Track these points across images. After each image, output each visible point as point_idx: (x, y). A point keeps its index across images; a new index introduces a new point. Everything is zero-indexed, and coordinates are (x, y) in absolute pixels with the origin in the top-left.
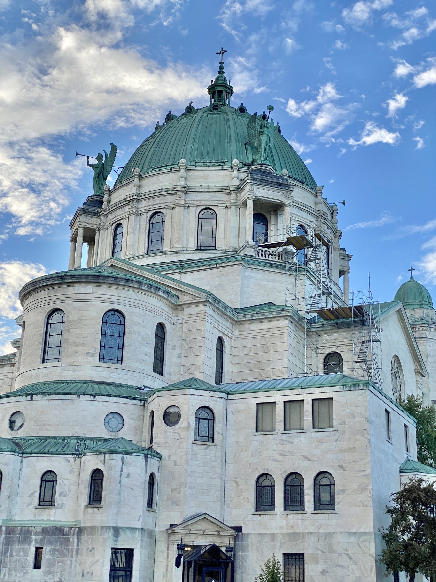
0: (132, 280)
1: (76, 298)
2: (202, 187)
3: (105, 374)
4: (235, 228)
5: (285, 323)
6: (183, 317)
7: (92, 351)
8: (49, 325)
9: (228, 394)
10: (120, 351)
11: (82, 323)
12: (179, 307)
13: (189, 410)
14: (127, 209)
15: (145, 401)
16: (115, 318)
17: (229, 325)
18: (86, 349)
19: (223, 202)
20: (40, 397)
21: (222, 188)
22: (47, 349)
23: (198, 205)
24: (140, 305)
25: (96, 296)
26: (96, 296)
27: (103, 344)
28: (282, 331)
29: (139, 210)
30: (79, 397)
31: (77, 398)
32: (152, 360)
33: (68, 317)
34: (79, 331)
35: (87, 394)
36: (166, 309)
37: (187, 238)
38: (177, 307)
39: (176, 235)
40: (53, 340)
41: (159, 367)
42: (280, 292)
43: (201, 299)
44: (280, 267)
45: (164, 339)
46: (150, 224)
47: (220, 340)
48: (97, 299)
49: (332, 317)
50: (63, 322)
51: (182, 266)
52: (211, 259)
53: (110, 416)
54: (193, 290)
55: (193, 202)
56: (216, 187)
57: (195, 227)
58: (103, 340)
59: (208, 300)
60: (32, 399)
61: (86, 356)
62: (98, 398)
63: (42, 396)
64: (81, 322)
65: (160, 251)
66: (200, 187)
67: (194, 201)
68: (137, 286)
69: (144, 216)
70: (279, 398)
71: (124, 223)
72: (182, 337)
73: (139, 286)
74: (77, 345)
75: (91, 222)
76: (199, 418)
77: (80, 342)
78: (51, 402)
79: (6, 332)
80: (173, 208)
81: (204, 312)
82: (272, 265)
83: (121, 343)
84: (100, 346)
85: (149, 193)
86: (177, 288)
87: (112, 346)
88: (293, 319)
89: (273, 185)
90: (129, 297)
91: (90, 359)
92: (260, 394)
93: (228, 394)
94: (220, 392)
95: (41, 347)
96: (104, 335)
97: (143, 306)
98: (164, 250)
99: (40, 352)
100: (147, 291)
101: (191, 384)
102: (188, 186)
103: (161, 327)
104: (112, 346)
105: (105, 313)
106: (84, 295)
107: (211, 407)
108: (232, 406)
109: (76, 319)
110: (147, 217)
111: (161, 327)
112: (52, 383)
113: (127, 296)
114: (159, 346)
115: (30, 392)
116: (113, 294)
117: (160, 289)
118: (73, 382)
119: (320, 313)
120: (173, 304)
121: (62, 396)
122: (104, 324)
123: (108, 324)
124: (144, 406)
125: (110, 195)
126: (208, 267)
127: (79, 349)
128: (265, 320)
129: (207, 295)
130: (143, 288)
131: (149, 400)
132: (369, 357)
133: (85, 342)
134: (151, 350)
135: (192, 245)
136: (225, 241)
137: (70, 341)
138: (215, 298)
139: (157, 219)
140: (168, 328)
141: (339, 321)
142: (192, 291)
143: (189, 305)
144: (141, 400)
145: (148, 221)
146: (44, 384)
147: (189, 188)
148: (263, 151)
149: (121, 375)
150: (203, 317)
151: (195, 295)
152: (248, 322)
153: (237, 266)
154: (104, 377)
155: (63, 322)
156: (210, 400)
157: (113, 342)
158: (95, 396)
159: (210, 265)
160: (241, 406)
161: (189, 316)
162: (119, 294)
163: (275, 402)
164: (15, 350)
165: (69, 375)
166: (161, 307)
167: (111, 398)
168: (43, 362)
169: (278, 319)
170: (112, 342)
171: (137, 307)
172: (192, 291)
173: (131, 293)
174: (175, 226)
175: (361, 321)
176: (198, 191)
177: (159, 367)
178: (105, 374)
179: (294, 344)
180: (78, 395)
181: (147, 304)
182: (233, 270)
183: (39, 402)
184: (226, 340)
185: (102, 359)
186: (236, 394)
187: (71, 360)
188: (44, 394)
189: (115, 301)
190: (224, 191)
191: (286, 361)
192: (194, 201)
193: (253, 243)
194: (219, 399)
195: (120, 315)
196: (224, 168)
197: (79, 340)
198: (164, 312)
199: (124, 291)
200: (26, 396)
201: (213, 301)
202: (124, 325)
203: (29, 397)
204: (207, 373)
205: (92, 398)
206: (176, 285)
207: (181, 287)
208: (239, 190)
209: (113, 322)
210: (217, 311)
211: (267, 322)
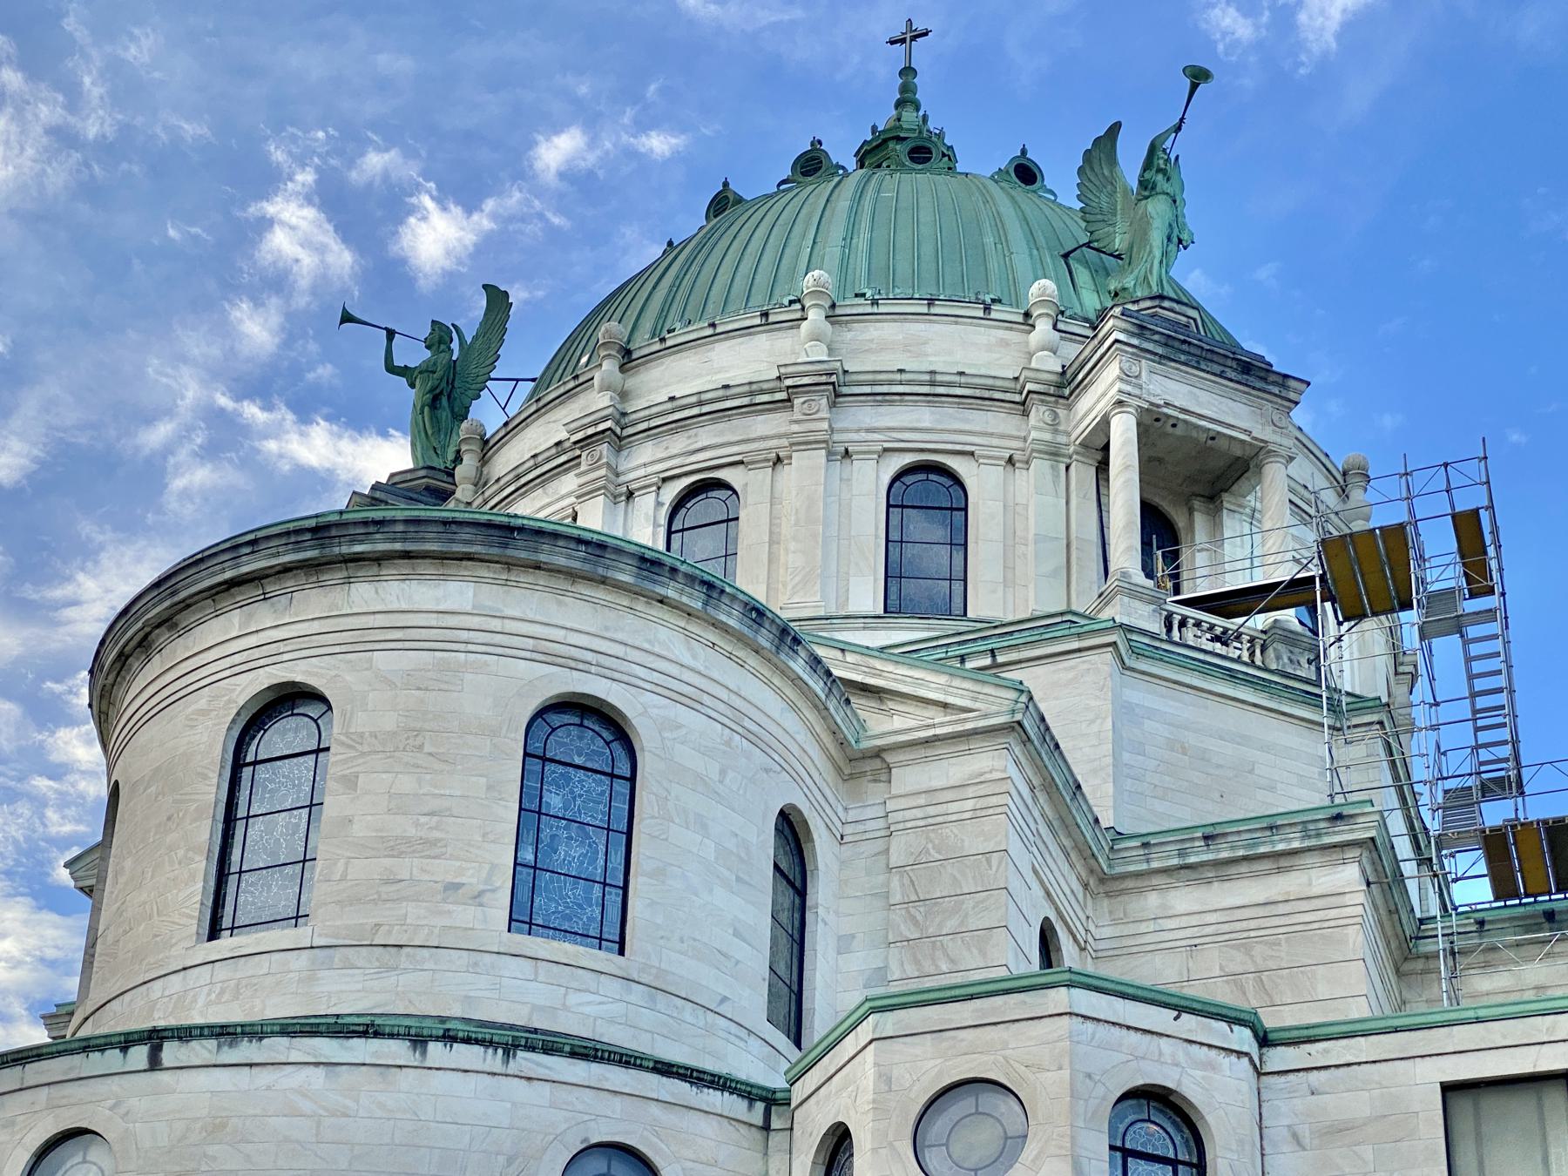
0: (674, 570)
1: (401, 634)
2: (905, 377)
6: (891, 806)
7: (474, 881)
11: (421, 747)
18: (443, 870)
19: (995, 442)
20: (202, 1050)
21: (990, 382)
22: (233, 879)
23: (886, 450)
24: (706, 699)
25: (495, 624)
26: (495, 624)
27: (528, 856)
29: (622, 479)
30: (424, 1053)
34: (406, 783)
35: (467, 1041)
43: (986, 716)
45: (802, 893)
46: (670, 533)
48: (498, 639)
50: (318, 751)
54: (943, 679)
55: (864, 436)
56: (963, 379)
57: (877, 537)
59: (1018, 717)
60: (155, 1064)
61: (444, 901)
62: (525, 1061)
64: (417, 743)
66: (898, 377)
67: (868, 430)
69: (645, 502)
72: (887, 895)
73: (706, 604)
76: (1127, 1153)
77: (412, 832)
78: (264, 1077)
80: (779, 460)
83: (617, 859)
84: (516, 864)
85: (669, 406)
86: (859, 678)
89: (1217, 369)
90: (657, 650)
91: (465, 915)
96: (531, 813)
97: (721, 707)
100: (740, 638)
102: (846, 372)
105: (541, 713)
108: (1290, 1104)
110: (659, 504)
113: (646, 646)
116: (576, 626)
120: (843, 744)
121: (326, 1047)
122: (535, 765)
123: (549, 767)
124: (766, 1127)
125: (484, 460)
127: (406, 867)
129: (1013, 695)
130: (723, 618)
133: (436, 834)
137: (358, 830)
140: (823, 850)
143: (922, 752)
145: (663, 520)
147: (848, 378)
148: (1157, 253)
150: (994, 800)
151: (950, 700)
154: (535, 1008)
155: (318, 751)
156: (1181, 1057)
158: (510, 1049)
161: (922, 800)
162: (607, 629)
170: (570, 853)
173: (663, 634)
174: (786, 529)
176: (885, 392)
180: (419, 1041)
181: (738, 703)
182: (1071, 675)
185: (522, 919)
189: (589, 656)
190: (997, 395)
192: (868, 430)
196: (993, 315)
197: (404, 826)
198: (808, 764)
200: (124, 1050)
202: (632, 779)
203: (140, 1054)
205: (494, 1060)
208: (1067, 392)
209: (578, 761)
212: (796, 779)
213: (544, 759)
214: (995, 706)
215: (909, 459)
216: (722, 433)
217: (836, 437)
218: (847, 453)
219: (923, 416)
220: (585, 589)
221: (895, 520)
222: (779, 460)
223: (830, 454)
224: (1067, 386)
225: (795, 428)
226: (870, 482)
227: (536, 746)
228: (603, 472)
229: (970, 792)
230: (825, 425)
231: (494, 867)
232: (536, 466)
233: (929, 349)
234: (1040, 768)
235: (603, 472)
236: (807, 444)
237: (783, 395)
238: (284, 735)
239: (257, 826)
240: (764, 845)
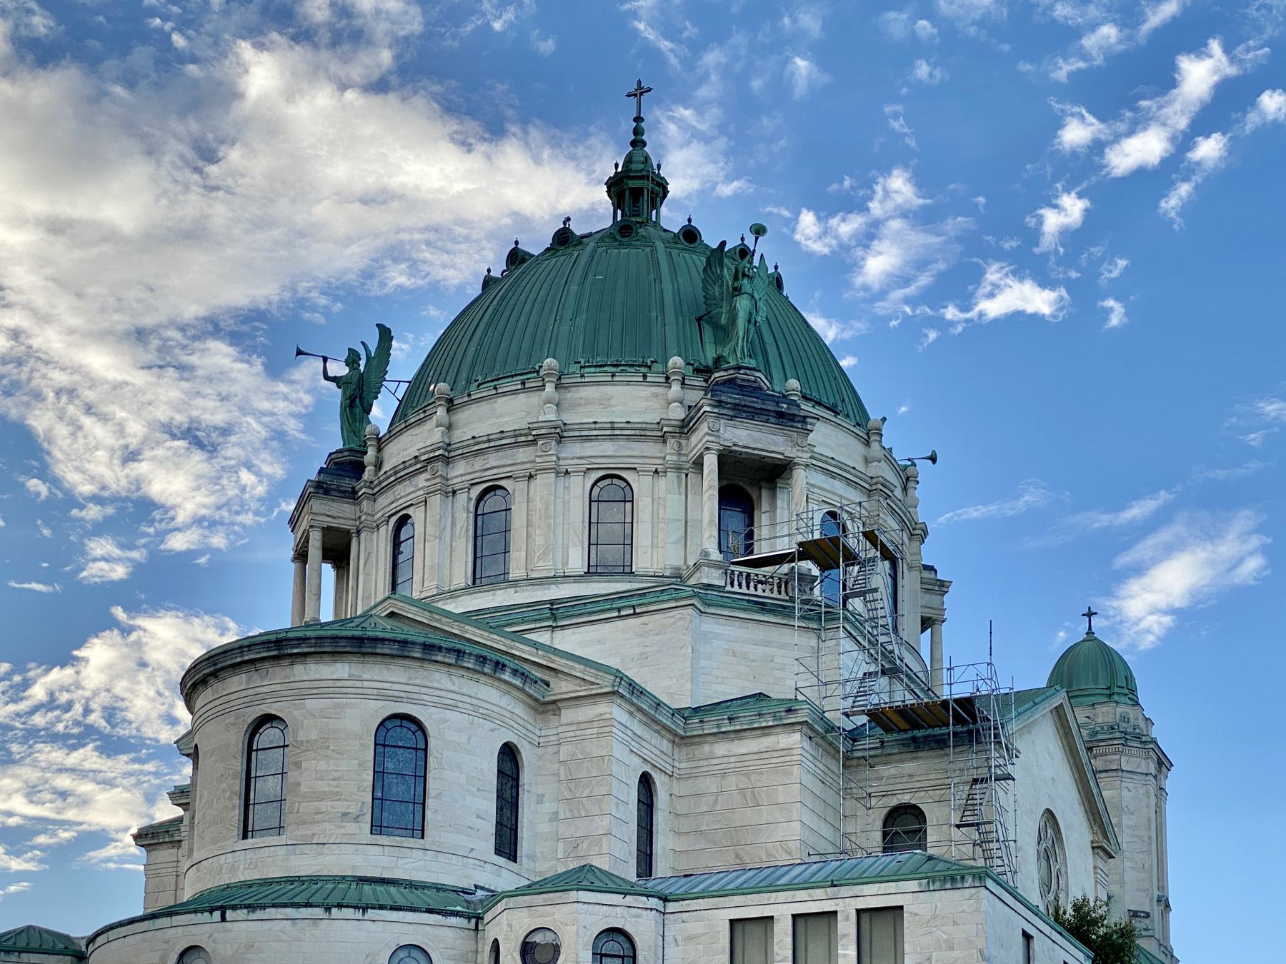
3: (385, 861)
4: (676, 523)
5: (794, 739)
6: (560, 729)
8: (254, 754)
9: (665, 900)
10: (419, 808)
12: (551, 707)
13: (578, 935)
14: (422, 480)
15: (479, 918)
16: (404, 735)
17: (666, 745)
18: (341, 807)
19: (647, 461)
20: (242, 914)
24: (460, 704)
25: (359, 684)
26: (359, 684)
27: (379, 794)
28: (788, 758)
31: (326, 916)
32: (491, 828)
33: (295, 733)
35: (347, 907)
36: (520, 710)
37: (566, 549)
38: (546, 707)
39: (539, 540)
40: (266, 787)
41: (507, 844)
42: (782, 669)
44: (783, 610)
45: (517, 780)
46: (476, 515)
47: (646, 782)
48: (360, 691)
49: (903, 724)
50: (284, 746)
51: (555, 613)
52: (621, 596)
53: (402, 954)
54: (582, 667)
55: (576, 461)
58: (379, 785)
62: (371, 913)
63: (245, 911)
65: (503, 580)
68: (453, 661)
69: (462, 498)
70: (782, 908)
71: (417, 514)
74: (321, 797)
75: (338, 513)
76: (602, 955)
77: (326, 789)
79: (157, 774)
81: (608, 716)
82: (762, 607)
87: (399, 794)
88: (812, 729)
91: (351, 827)
92: (738, 900)
93: (665, 900)
94: (648, 896)
95: (238, 802)
98: (512, 576)
99: (236, 814)
101: (584, 879)
103: (509, 754)
104: (399, 794)
105: (381, 724)
106: (330, 683)
107: (629, 928)
109: (315, 737)
110: (470, 499)
111: (509, 754)
112: (267, 882)
114: (507, 795)
115: (220, 903)
117: (504, 666)
118: (314, 879)
119: (876, 716)
120: (536, 700)
121: (290, 912)
122: (380, 749)
126: (616, 614)
127: (324, 805)
128: (748, 733)
130: (466, 665)
131: (488, 917)
132: (987, 813)
134: (489, 805)
135: (577, 562)
136: (654, 553)
137: (303, 789)
138: (632, 685)
139: (492, 502)
140: (527, 755)
141: (919, 733)
142: (578, 670)
144: (469, 918)
145: (472, 509)
146: (248, 885)
149: (422, 863)
152: (708, 739)
153: (682, 611)
157: (402, 788)
158: (365, 909)
159: (619, 610)
160: (695, 926)
161: (574, 727)
163: (772, 917)
164: (179, 812)
165: (304, 864)
166: (510, 708)
167: (401, 913)
168: (245, 837)
169: (779, 730)
170: (398, 789)
171: (452, 708)
172: (578, 670)
175: (970, 732)
177: (507, 844)
178: (385, 861)
179: (818, 788)
180: (328, 909)
181: (475, 702)
183: (241, 926)
184: (658, 778)
185: (377, 827)
186: (683, 900)
187: (304, 831)
188: (248, 907)
189: (403, 694)
191: (797, 825)
193: (719, 557)
194: (644, 913)
195: (414, 727)
197: (323, 786)
199: (421, 672)
201: (629, 691)
202: (426, 750)
203: (217, 914)
204: (617, 855)
205: (359, 915)
206: (542, 657)
207: (553, 662)
210: (638, 715)
211: (754, 737)
212: (511, 728)
213: (384, 746)
214: (606, 684)
215: (601, 473)
216: (501, 458)
217: (561, 462)
218: (567, 472)
219: (608, 448)
220: (401, 662)
221: (594, 510)
222: (531, 477)
223: (557, 473)
224: (685, 428)
225: (538, 460)
226: (579, 487)
227: (381, 740)
228: (438, 480)
229: (595, 724)
230: (554, 458)
231: (363, 803)
232: (405, 468)
233: (613, 402)
234: (633, 704)
235: (438, 480)
236: (545, 470)
237: (530, 438)
238: (269, 735)
239: (260, 781)
240: (489, 767)
